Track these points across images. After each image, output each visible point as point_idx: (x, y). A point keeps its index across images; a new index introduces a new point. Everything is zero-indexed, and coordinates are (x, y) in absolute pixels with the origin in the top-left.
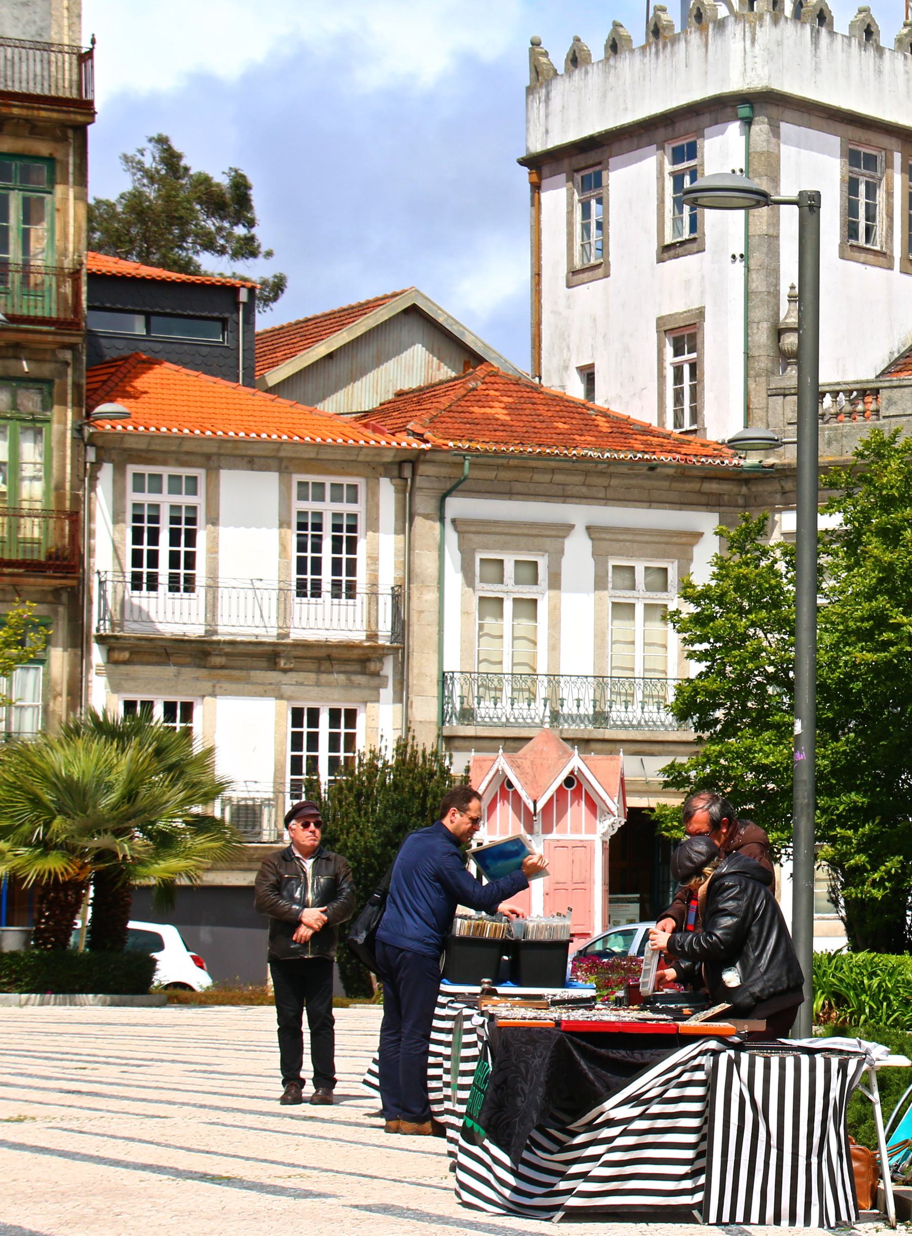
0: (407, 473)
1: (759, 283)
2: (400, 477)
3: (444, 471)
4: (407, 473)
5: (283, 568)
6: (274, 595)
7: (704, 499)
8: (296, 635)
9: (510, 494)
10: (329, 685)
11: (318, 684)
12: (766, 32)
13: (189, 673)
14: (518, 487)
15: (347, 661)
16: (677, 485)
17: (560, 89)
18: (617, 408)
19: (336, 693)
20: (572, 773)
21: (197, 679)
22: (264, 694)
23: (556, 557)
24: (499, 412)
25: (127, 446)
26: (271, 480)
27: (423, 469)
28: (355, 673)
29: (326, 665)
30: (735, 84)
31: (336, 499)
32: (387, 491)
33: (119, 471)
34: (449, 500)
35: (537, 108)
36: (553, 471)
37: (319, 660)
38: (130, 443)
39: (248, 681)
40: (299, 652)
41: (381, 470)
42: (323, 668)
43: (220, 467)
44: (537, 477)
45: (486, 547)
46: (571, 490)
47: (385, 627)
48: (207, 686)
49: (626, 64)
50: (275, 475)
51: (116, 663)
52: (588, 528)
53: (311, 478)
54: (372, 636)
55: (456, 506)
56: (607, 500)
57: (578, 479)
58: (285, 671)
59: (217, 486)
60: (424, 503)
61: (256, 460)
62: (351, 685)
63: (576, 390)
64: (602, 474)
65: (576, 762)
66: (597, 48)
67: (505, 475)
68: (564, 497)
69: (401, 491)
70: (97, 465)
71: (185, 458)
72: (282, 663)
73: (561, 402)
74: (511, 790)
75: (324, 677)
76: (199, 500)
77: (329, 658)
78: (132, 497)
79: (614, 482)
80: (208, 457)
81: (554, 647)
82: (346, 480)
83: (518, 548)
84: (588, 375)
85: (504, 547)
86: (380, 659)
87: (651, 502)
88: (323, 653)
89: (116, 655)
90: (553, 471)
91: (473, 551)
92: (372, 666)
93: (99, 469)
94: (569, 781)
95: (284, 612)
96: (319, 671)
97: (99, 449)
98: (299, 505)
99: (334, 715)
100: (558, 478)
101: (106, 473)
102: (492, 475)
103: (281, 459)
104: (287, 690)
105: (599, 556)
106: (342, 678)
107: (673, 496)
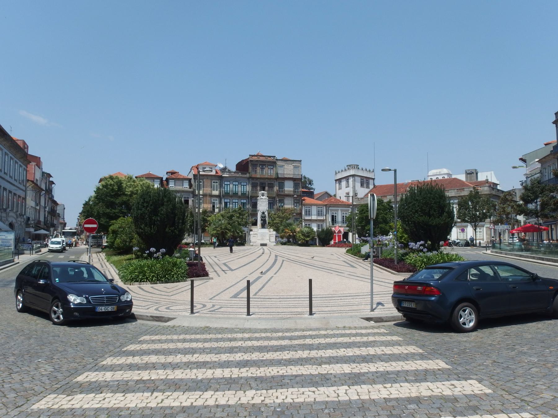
1: (354, 190)
12: (354, 170)
17: (337, 174)
18: (343, 200)
23: (338, 212)
26: (316, 206)
30: (352, 174)
32: (325, 207)
35: (336, 176)
47: (325, 219)
49: (343, 172)
55: (330, 208)
60: (327, 208)
63: (339, 199)
66: (341, 171)
68: (338, 207)
73: (338, 200)
76: (310, 208)
78: (305, 208)
81: (338, 219)
84: (340, 197)
101: (303, 207)
105: (341, 212)
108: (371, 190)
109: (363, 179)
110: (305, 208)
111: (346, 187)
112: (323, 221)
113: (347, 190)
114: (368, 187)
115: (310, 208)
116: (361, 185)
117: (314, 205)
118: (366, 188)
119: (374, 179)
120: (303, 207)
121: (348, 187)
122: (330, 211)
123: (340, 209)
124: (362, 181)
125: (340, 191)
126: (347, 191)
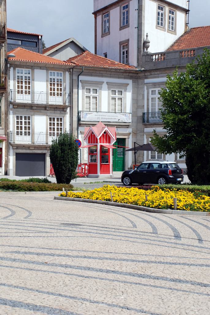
0: (71, 71)
2: (70, 71)
3: (78, 70)
4: (71, 71)
5: (47, 89)
6: (45, 95)
7: (129, 77)
8: (50, 103)
9: (92, 75)
10: (57, 113)
11: (54, 113)
13: (29, 110)
14: (93, 74)
15: (60, 108)
16: (124, 74)
19: (58, 115)
20: (105, 131)
21: (31, 112)
22: (44, 115)
24: (89, 59)
25: (15, 64)
26: (44, 72)
27: (74, 70)
28: (62, 111)
29: (56, 109)
31: (58, 76)
32: (67, 74)
33: (14, 69)
34: (79, 76)
36: (100, 71)
37: (54, 108)
38: (17, 63)
39: (41, 112)
40: (50, 106)
41: (66, 70)
42: (55, 110)
43: (34, 69)
44: (97, 72)
45: (87, 86)
46: (103, 75)
48: (32, 113)
50: (46, 70)
51: (15, 108)
52: (107, 82)
53: (52, 71)
54: (65, 103)
55: (81, 78)
56: (110, 77)
57: (105, 72)
58: (48, 110)
59: (34, 72)
60: (75, 78)
61: (41, 67)
62: (61, 113)
64: (110, 71)
65: (106, 129)
67: (91, 71)
68: (102, 76)
69: (70, 74)
70: (10, 67)
71: (27, 67)
72: (47, 109)
74: (93, 134)
75: (55, 112)
77: (56, 108)
79: (112, 73)
80: (32, 66)
82: (59, 72)
83: (93, 86)
85: (90, 86)
86: (67, 108)
87: (119, 78)
88: (55, 106)
89: (14, 106)
90: (100, 71)
91: (84, 87)
92: (65, 110)
93: (10, 68)
94: (105, 133)
95: (47, 99)
96: (55, 110)
97: (10, 64)
98: (50, 77)
99: (58, 119)
100: (101, 72)
101: (12, 69)
102: (88, 71)
103: (46, 67)
104: (48, 114)
106: (59, 112)
107: (123, 76)
108: (179, 39)
109: (162, 9)
110: (17, 75)
111: (121, 28)
112: (62, 109)
113: (124, 35)
114: (173, 29)
115: (30, 75)
116: (158, 24)
117: (41, 68)
118: (169, 31)
119: (186, 11)
120: (12, 69)
121: (128, 26)
122: (80, 84)
123: (105, 80)
124: (161, 12)
125: (106, 38)
126: (123, 39)
